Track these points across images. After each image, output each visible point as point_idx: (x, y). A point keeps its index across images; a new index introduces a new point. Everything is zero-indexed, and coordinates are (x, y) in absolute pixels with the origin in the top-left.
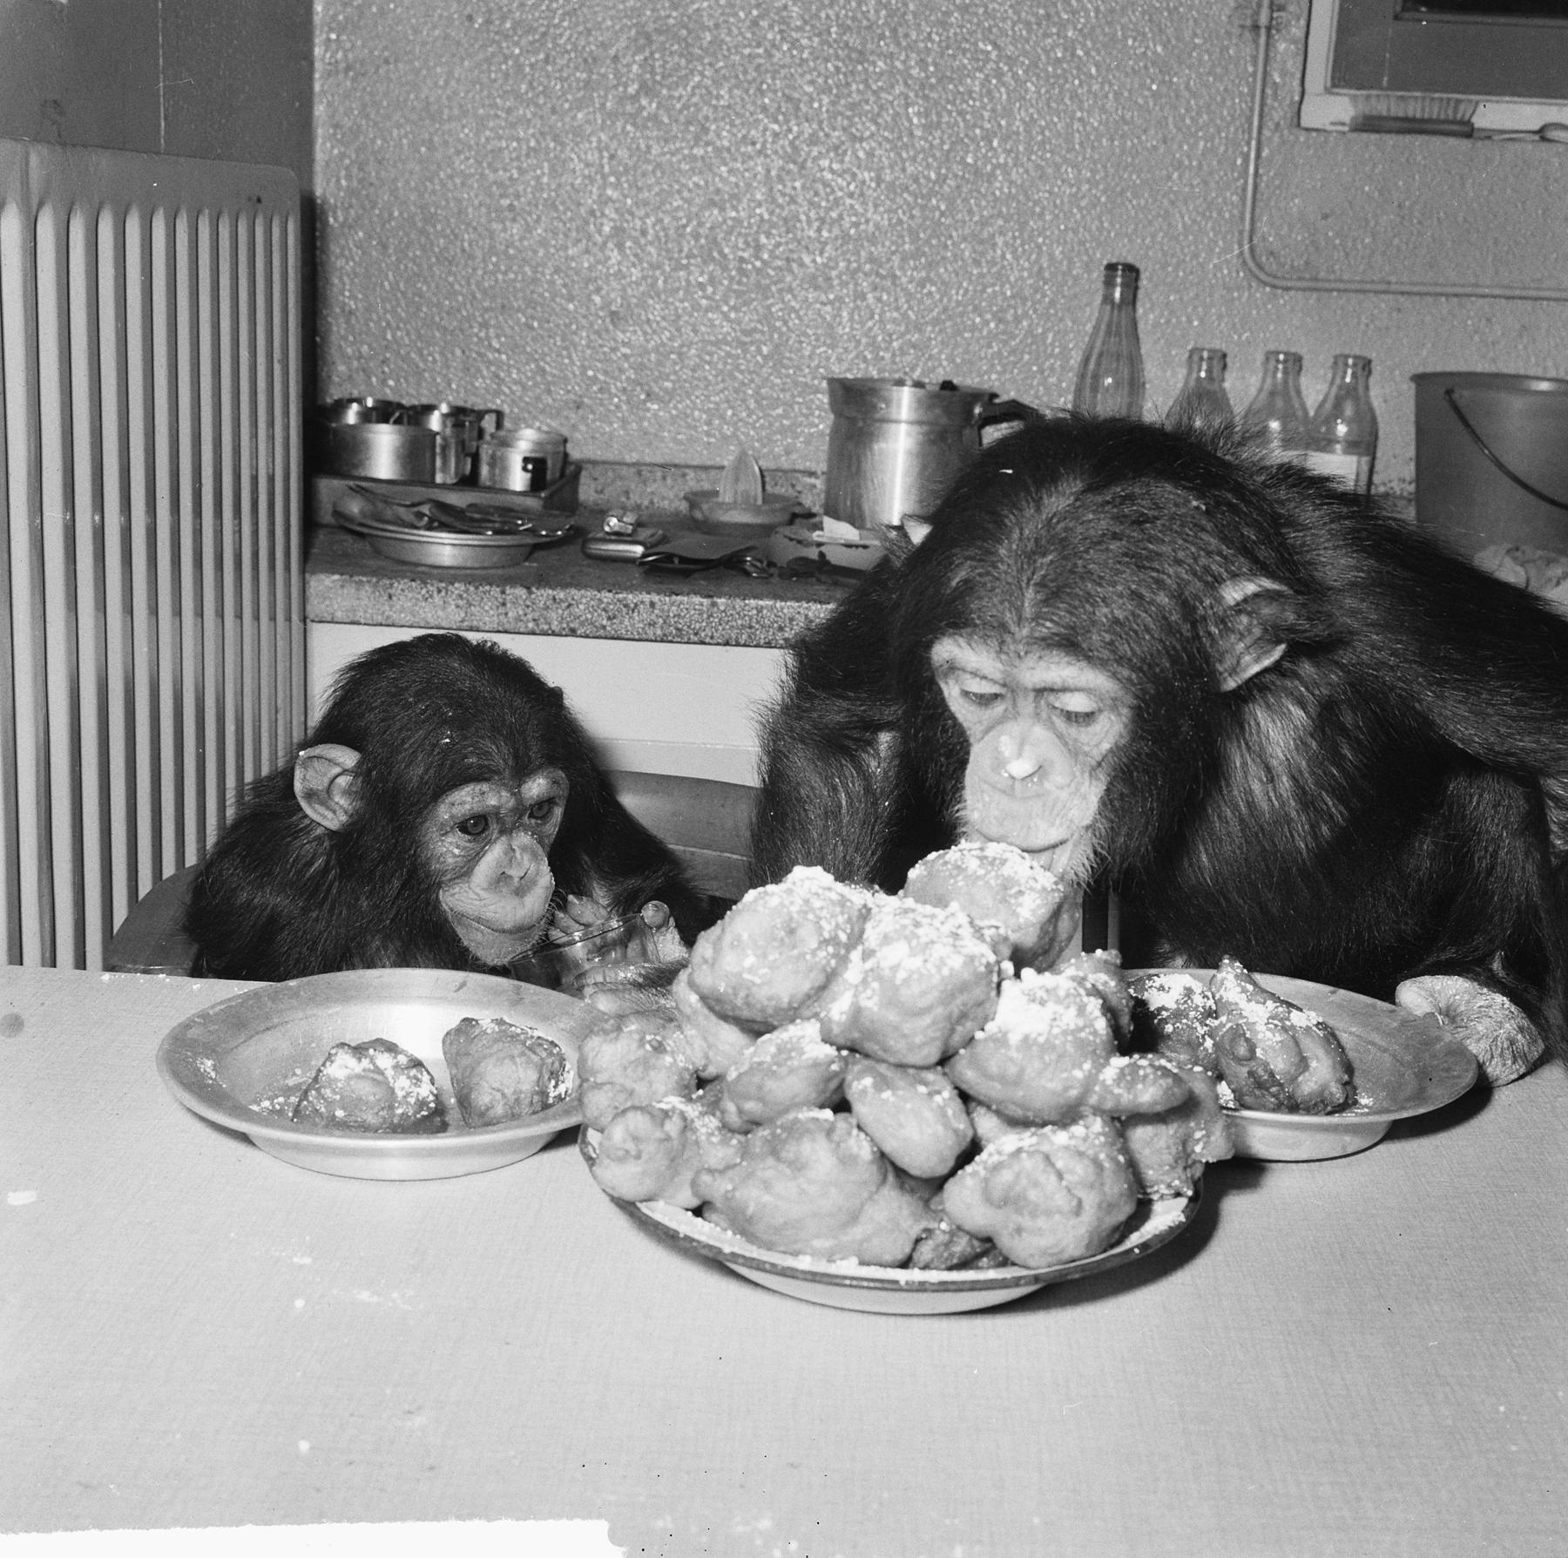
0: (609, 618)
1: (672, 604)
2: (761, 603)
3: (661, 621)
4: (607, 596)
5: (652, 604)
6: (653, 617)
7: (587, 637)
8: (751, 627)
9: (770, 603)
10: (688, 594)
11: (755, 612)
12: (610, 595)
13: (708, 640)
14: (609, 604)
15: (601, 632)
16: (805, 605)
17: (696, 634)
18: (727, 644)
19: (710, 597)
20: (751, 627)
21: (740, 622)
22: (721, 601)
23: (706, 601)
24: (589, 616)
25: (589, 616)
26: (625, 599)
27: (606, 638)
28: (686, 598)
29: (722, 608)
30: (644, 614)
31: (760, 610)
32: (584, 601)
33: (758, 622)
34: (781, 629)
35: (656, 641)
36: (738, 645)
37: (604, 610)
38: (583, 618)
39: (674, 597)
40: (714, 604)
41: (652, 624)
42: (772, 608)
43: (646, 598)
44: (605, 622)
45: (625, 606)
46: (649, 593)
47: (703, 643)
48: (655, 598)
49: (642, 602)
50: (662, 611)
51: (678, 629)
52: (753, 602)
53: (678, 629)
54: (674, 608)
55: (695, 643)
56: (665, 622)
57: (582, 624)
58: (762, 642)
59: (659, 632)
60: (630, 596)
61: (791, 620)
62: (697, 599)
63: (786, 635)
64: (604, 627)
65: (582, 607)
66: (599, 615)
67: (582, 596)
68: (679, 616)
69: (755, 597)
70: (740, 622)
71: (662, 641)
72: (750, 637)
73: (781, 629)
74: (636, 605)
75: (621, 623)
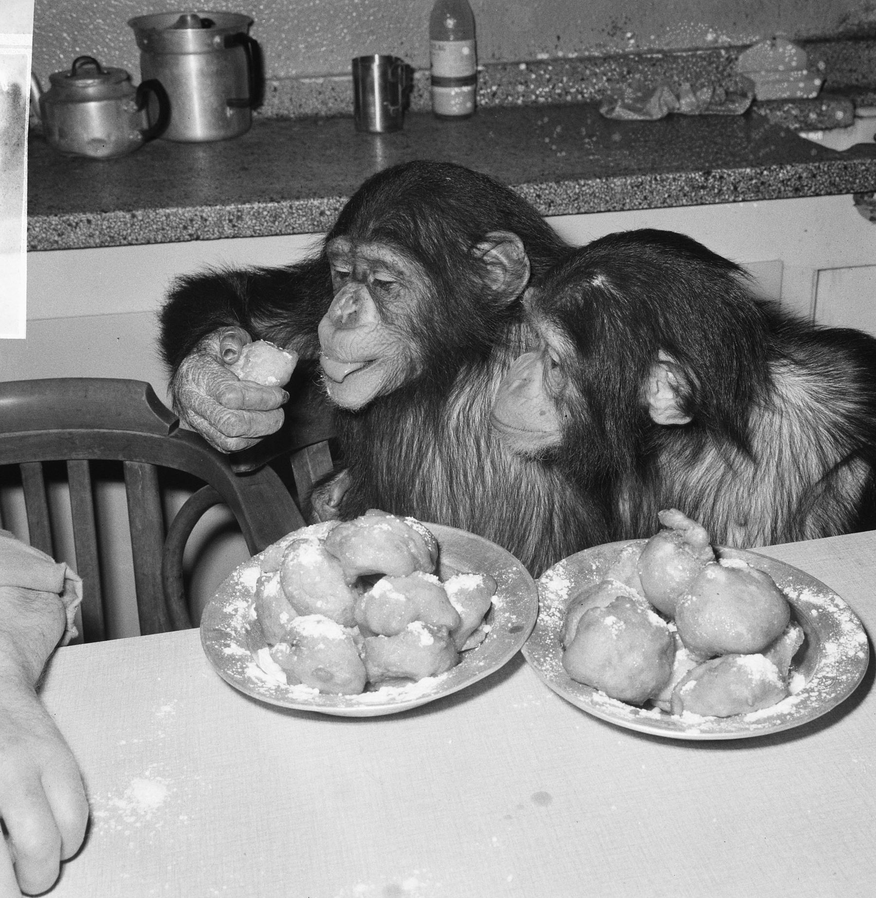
0: (59, 235)
1: (103, 220)
2: (168, 211)
3: (97, 233)
4: (54, 220)
5: (89, 221)
6: (91, 230)
7: (45, 250)
8: (163, 229)
9: (174, 210)
10: (114, 211)
11: (164, 218)
12: (57, 218)
13: (134, 242)
14: (57, 225)
15: (55, 246)
16: (200, 209)
17: (125, 239)
18: (148, 243)
19: (129, 211)
20: (163, 229)
21: (155, 226)
22: (139, 213)
23: (128, 216)
24: (44, 235)
25: (44, 235)
26: (68, 220)
27: (59, 249)
28: (113, 214)
29: (140, 218)
30: (84, 229)
31: (168, 216)
32: (38, 225)
33: (168, 225)
34: (185, 228)
35: (96, 247)
36: (156, 242)
37: (54, 229)
38: (40, 237)
39: (104, 214)
40: (134, 216)
41: (91, 236)
42: (175, 215)
43: (83, 217)
44: (56, 238)
45: (70, 225)
46: (84, 213)
47: (130, 244)
48: (90, 216)
49: (81, 221)
50: (97, 225)
51: (110, 237)
52: (161, 211)
53: (110, 237)
54: (105, 223)
55: (125, 245)
56: (100, 233)
57: (39, 241)
58: (173, 239)
59: (98, 241)
60: (72, 218)
61: (192, 220)
62: (120, 214)
63: (190, 231)
64: (57, 242)
65: (37, 229)
66: (52, 234)
67: (37, 222)
68: (109, 227)
69: (163, 207)
70: (155, 226)
71: (101, 246)
72: (164, 236)
73: (185, 228)
74: (77, 224)
75: (69, 237)
